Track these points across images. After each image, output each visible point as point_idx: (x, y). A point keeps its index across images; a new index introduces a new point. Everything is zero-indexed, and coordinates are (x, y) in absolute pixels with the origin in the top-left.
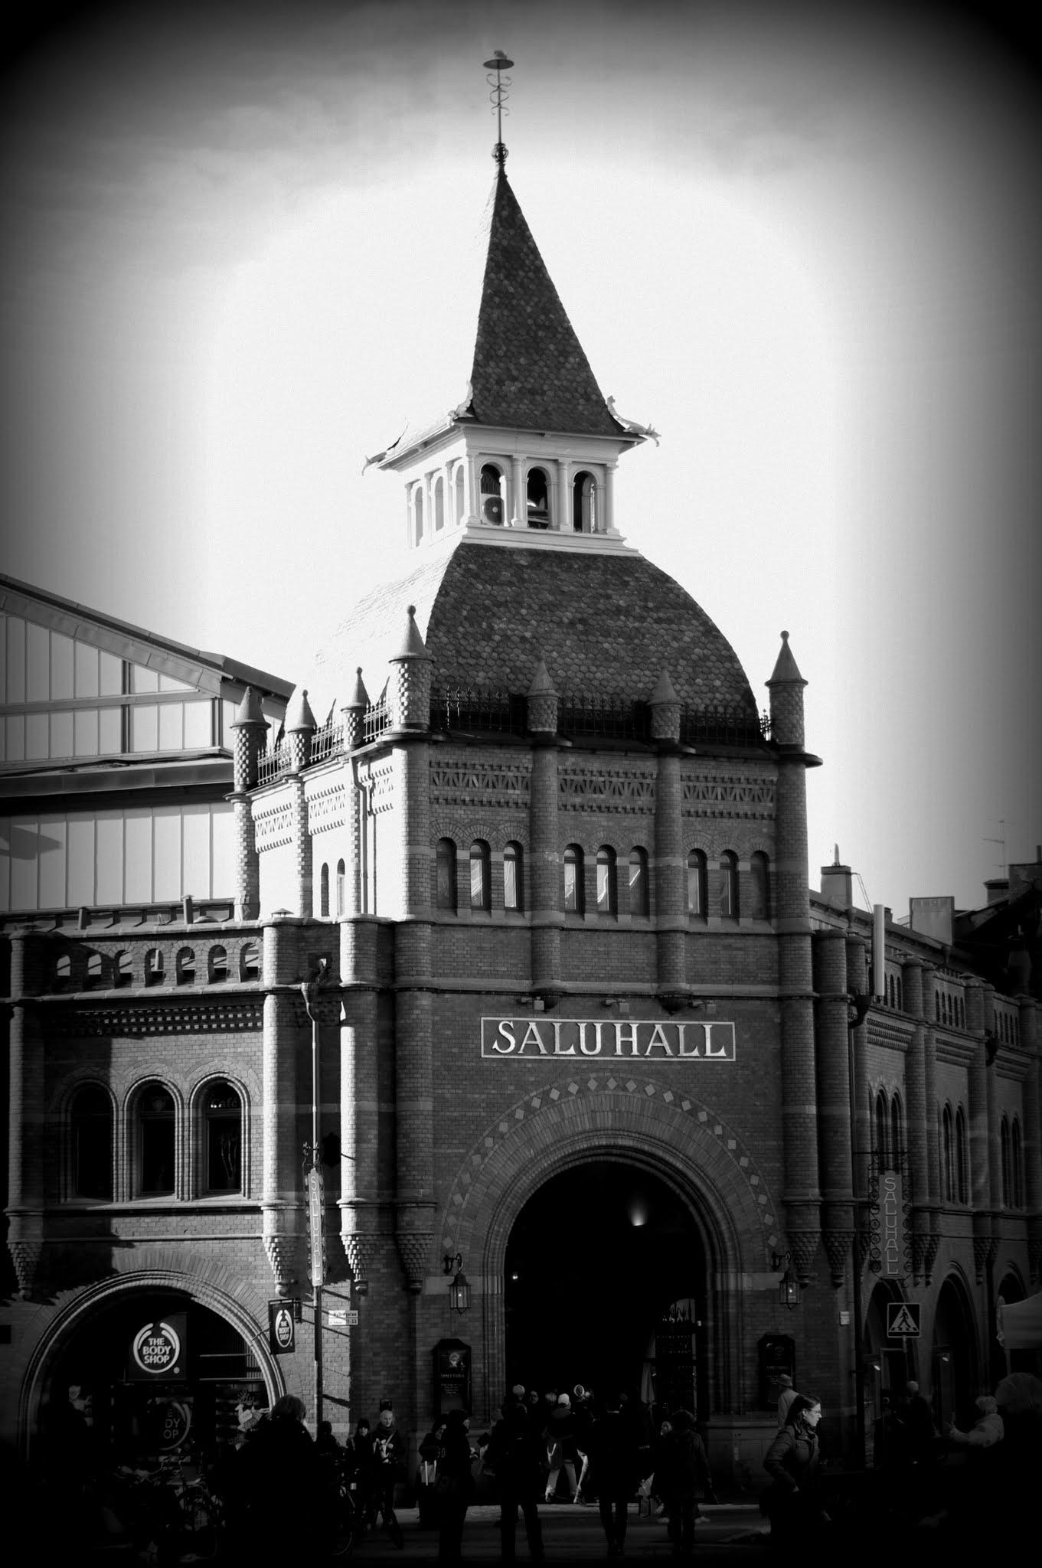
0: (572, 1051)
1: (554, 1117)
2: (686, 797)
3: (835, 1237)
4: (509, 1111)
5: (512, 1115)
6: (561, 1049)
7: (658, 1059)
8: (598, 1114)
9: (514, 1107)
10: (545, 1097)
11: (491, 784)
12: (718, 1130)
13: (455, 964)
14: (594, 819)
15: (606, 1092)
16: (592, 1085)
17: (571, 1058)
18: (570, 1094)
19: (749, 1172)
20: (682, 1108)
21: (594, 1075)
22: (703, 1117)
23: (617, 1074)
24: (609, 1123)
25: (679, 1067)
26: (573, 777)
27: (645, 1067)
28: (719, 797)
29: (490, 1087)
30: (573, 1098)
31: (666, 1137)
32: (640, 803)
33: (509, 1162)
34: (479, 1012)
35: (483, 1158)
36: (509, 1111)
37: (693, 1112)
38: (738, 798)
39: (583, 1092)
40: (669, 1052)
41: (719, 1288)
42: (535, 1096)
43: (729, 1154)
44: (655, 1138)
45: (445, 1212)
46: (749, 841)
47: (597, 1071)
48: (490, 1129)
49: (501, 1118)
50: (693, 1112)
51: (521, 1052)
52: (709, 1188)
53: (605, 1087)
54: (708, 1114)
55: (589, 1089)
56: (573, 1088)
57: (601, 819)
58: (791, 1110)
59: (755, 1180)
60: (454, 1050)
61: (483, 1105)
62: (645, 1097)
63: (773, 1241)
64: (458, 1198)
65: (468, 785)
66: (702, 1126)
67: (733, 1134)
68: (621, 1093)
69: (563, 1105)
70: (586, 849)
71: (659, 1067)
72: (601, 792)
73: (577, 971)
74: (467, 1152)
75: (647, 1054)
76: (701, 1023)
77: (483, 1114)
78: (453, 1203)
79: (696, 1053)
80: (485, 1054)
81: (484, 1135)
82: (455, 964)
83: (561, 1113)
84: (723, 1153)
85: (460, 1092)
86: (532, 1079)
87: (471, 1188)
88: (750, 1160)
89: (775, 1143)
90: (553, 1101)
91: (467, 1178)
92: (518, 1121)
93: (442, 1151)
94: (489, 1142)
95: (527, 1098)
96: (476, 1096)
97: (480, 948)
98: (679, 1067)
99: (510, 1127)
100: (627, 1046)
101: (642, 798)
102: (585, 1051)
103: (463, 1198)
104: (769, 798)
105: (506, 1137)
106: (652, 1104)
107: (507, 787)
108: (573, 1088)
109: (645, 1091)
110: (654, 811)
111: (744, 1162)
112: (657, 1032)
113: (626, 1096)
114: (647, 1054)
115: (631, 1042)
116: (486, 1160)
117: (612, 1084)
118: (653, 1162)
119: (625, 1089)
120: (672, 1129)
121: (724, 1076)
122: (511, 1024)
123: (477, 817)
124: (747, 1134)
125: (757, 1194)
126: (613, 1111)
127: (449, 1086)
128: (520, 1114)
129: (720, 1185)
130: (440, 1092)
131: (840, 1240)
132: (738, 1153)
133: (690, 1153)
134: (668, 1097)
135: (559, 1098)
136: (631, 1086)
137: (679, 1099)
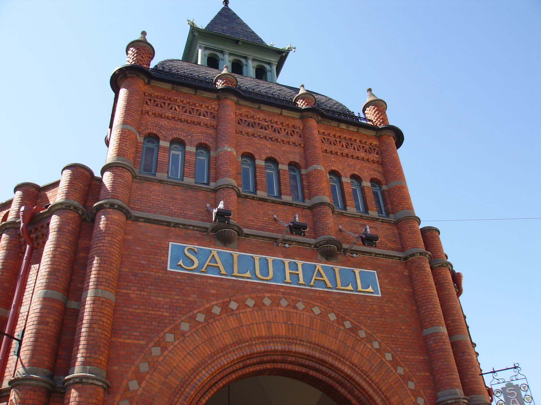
0: (248, 274)
1: (232, 323)
2: (323, 142)
4: (191, 314)
5: (194, 317)
7: (321, 289)
8: (273, 324)
9: (195, 312)
10: (225, 307)
13: (151, 204)
14: (261, 142)
15: (279, 308)
16: (267, 302)
17: (248, 280)
18: (247, 306)
19: (405, 378)
21: (269, 295)
22: (362, 334)
23: (288, 297)
24: (283, 332)
25: (338, 297)
27: (311, 294)
28: (345, 146)
29: (173, 293)
30: (250, 310)
31: (334, 347)
32: (293, 139)
33: (188, 356)
34: (168, 238)
35: (163, 350)
36: (191, 314)
37: (354, 330)
39: (259, 305)
43: (387, 363)
44: (324, 348)
45: (118, 397)
46: (367, 172)
47: (269, 292)
48: (171, 326)
49: (183, 319)
50: (354, 330)
52: (375, 390)
53: (279, 305)
54: (365, 332)
55: (264, 304)
56: (251, 303)
57: (269, 144)
58: (427, 331)
59: (411, 385)
60: (142, 262)
61: (167, 306)
62: (314, 316)
64: (133, 385)
66: (362, 341)
67: (388, 348)
68: (292, 310)
69: (241, 315)
70: (257, 156)
71: (322, 295)
72: (266, 129)
73: (251, 223)
74: (147, 344)
77: (167, 314)
78: (127, 389)
79: (350, 287)
80: (171, 267)
81: (166, 331)
82: (151, 204)
83: (240, 320)
84: (382, 363)
85: (145, 294)
86: (214, 292)
87: (148, 377)
88: (404, 370)
89: (422, 358)
90: (232, 310)
91: (144, 367)
92: (199, 323)
93: (122, 340)
94: (170, 338)
95: (208, 305)
96: (159, 299)
97: (173, 198)
98: (338, 297)
99: (192, 328)
104: (376, 152)
105: (186, 335)
106: (319, 321)
108: (251, 303)
109: (312, 311)
110: (302, 145)
111: (400, 370)
112: (318, 270)
113: (296, 313)
114: (312, 284)
115: (298, 274)
116: (166, 353)
117: (284, 303)
118: (324, 369)
119: (295, 307)
120: (338, 341)
121: (374, 307)
123: (177, 127)
125: (416, 397)
126: (286, 323)
127: (135, 289)
128: (201, 318)
129: (384, 389)
130: (125, 291)
132: (395, 363)
133: (355, 360)
134: (332, 317)
135: (237, 309)
136: (301, 306)
137: (341, 320)
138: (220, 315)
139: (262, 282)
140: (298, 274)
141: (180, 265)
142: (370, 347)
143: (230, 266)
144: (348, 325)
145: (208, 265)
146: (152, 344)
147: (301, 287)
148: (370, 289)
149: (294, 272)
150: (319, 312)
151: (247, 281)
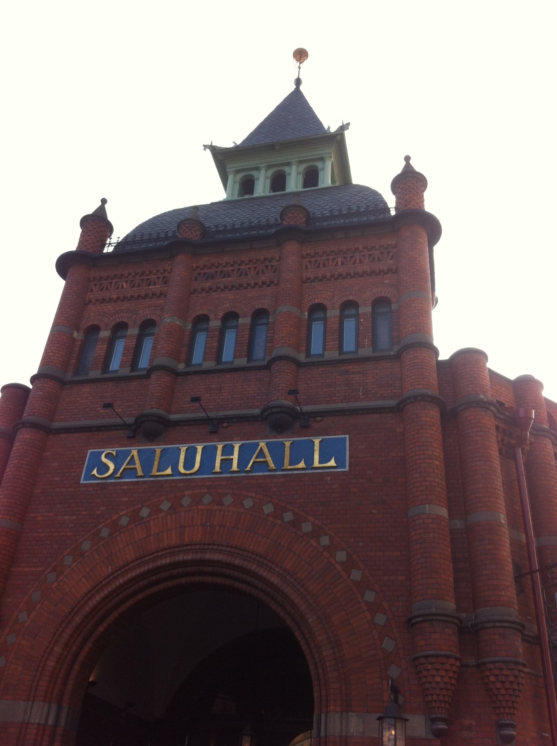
0: (169, 471)
3: (490, 670)
6: (158, 471)
7: (261, 474)
11: (136, 285)
12: (325, 541)
18: (161, 511)
20: (282, 519)
22: (307, 527)
26: (206, 271)
28: (340, 263)
38: (358, 261)
40: (272, 465)
41: (323, 734)
42: (125, 515)
43: (337, 566)
44: (249, 552)
51: (118, 475)
55: (182, 506)
56: (165, 506)
59: (370, 596)
60: (56, 479)
63: (394, 672)
64: (23, 616)
65: (117, 288)
68: (216, 507)
69: (151, 523)
75: (248, 468)
76: (311, 438)
77: (70, 534)
79: (302, 465)
81: (65, 553)
86: (125, 499)
90: (143, 518)
94: (68, 560)
100: (226, 463)
101: (266, 275)
102: (182, 470)
103: (29, 616)
107: (149, 285)
111: (356, 575)
112: (261, 448)
117: (207, 499)
119: (220, 503)
122: (114, 453)
124: (361, 544)
128: (105, 533)
131: (497, 672)
134: (268, 509)
135: (149, 516)
136: (228, 500)
138: (127, 526)
139: (185, 477)
140: (232, 459)
141: (94, 475)
142: (315, 544)
143: (147, 465)
144: (288, 517)
145: (124, 469)
146: (50, 569)
147: (234, 475)
148: (332, 463)
149: (227, 457)
150: (251, 504)
151: (167, 480)
